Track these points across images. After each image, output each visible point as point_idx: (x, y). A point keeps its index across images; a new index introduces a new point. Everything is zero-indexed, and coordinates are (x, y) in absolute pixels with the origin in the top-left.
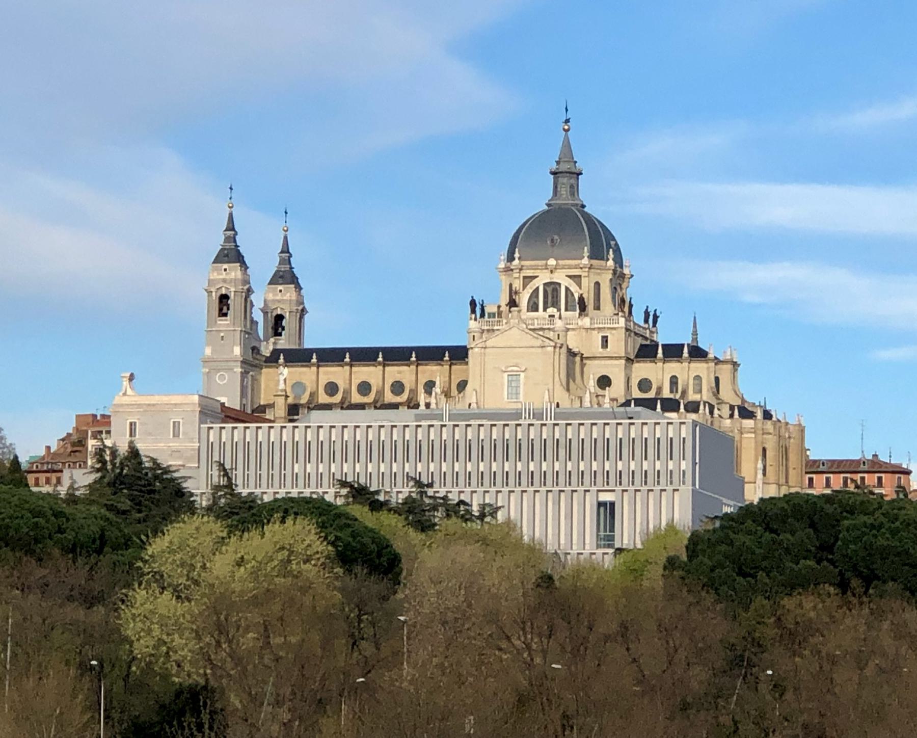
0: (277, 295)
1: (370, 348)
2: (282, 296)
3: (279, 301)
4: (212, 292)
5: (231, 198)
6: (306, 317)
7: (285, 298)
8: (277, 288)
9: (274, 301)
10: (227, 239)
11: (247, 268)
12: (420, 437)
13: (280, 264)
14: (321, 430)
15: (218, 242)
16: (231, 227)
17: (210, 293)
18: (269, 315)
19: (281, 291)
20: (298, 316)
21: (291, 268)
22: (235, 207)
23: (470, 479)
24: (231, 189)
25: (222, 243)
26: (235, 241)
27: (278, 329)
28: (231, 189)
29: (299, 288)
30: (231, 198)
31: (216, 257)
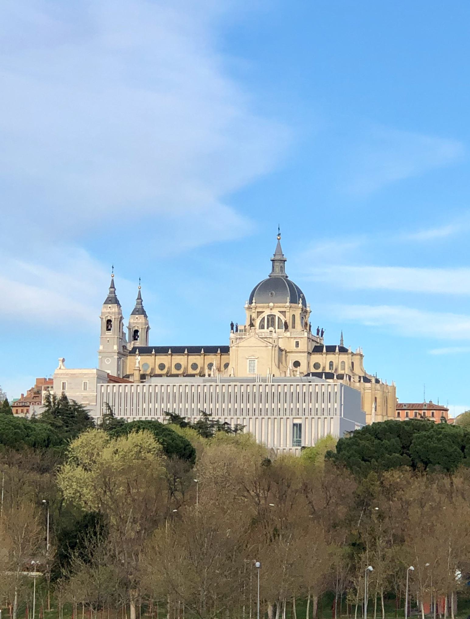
1: (208, 347)
3: (136, 323)
5: (113, 272)
6: (149, 331)
7: (139, 321)
9: (134, 323)
10: (111, 293)
12: (230, 391)
14: (236, 387)
16: (113, 286)
17: (102, 319)
18: (131, 330)
19: (137, 318)
21: (142, 307)
23: (304, 411)
24: (113, 267)
26: (115, 293)
28: (113, 267)
29: (146, 316)
30: (113, 272)
31: (106, 300)
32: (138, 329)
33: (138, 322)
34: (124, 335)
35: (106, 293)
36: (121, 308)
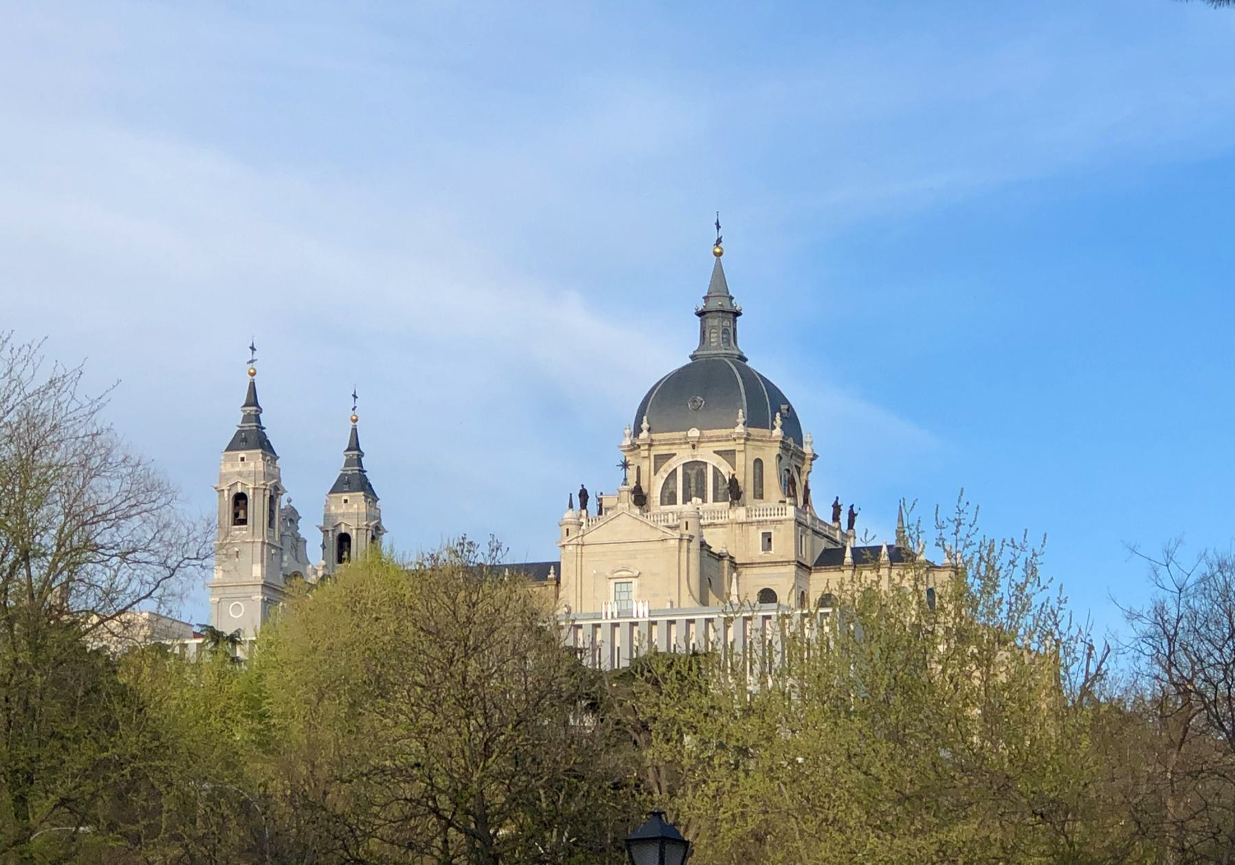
2: (347, 509)
3: (343, 515)
4: (327, 531)
5: (354, 409)
8: (341, 497)
11: (375, 499)
13: (345, 466)
16: (354, 445)
17: (326, 532)
18: (330, 533)
24: (355, 396)
26: (360, 464)
27: (342, 554)
28: (355, 396)
30: (354, 409)
31: (334, 486)
32: (348, 532)
33: (350, 511)
35: (336, 465)
36: (277, 461)
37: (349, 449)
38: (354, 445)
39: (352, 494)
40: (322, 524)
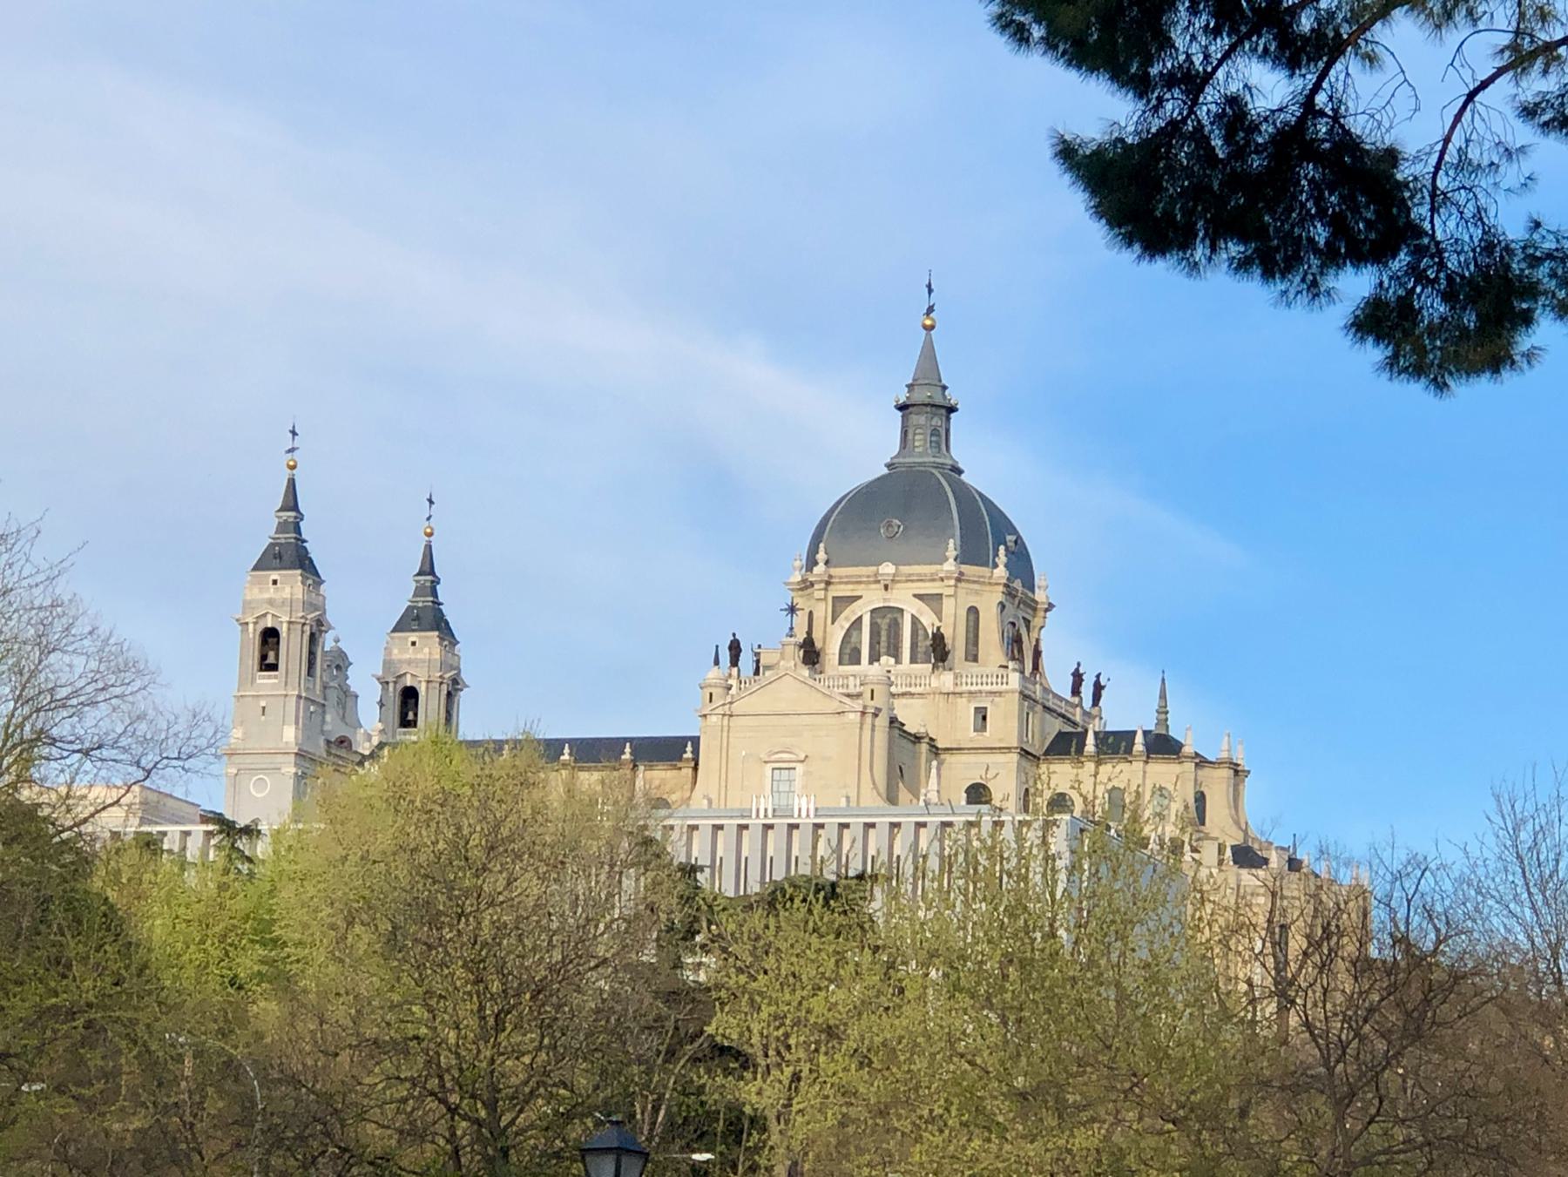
0: (407, 651)
3: (409, 662)
4: (387, 683)
5: (428, 519)
6: (464, 697)
8: (407, 638)
9: (400, 661)
10: (282, 527)
11: (454, 642)
13: (415, 595)
15: (264, 531)
16: (428, 568)
18: (391, 685)
19: (414, 644)
20: (445, 692)
22: (435, 533)
24: (431, 502)
25: (272, 533)
26: (434, 593)
27: (407, 714)
28: (431, 502)
30: (428, 519)
34: (350, 703)
35: (402, 597)
37: (419, 574)
38: (428, 568)
39: (423, 634)
40: (380, 673)
